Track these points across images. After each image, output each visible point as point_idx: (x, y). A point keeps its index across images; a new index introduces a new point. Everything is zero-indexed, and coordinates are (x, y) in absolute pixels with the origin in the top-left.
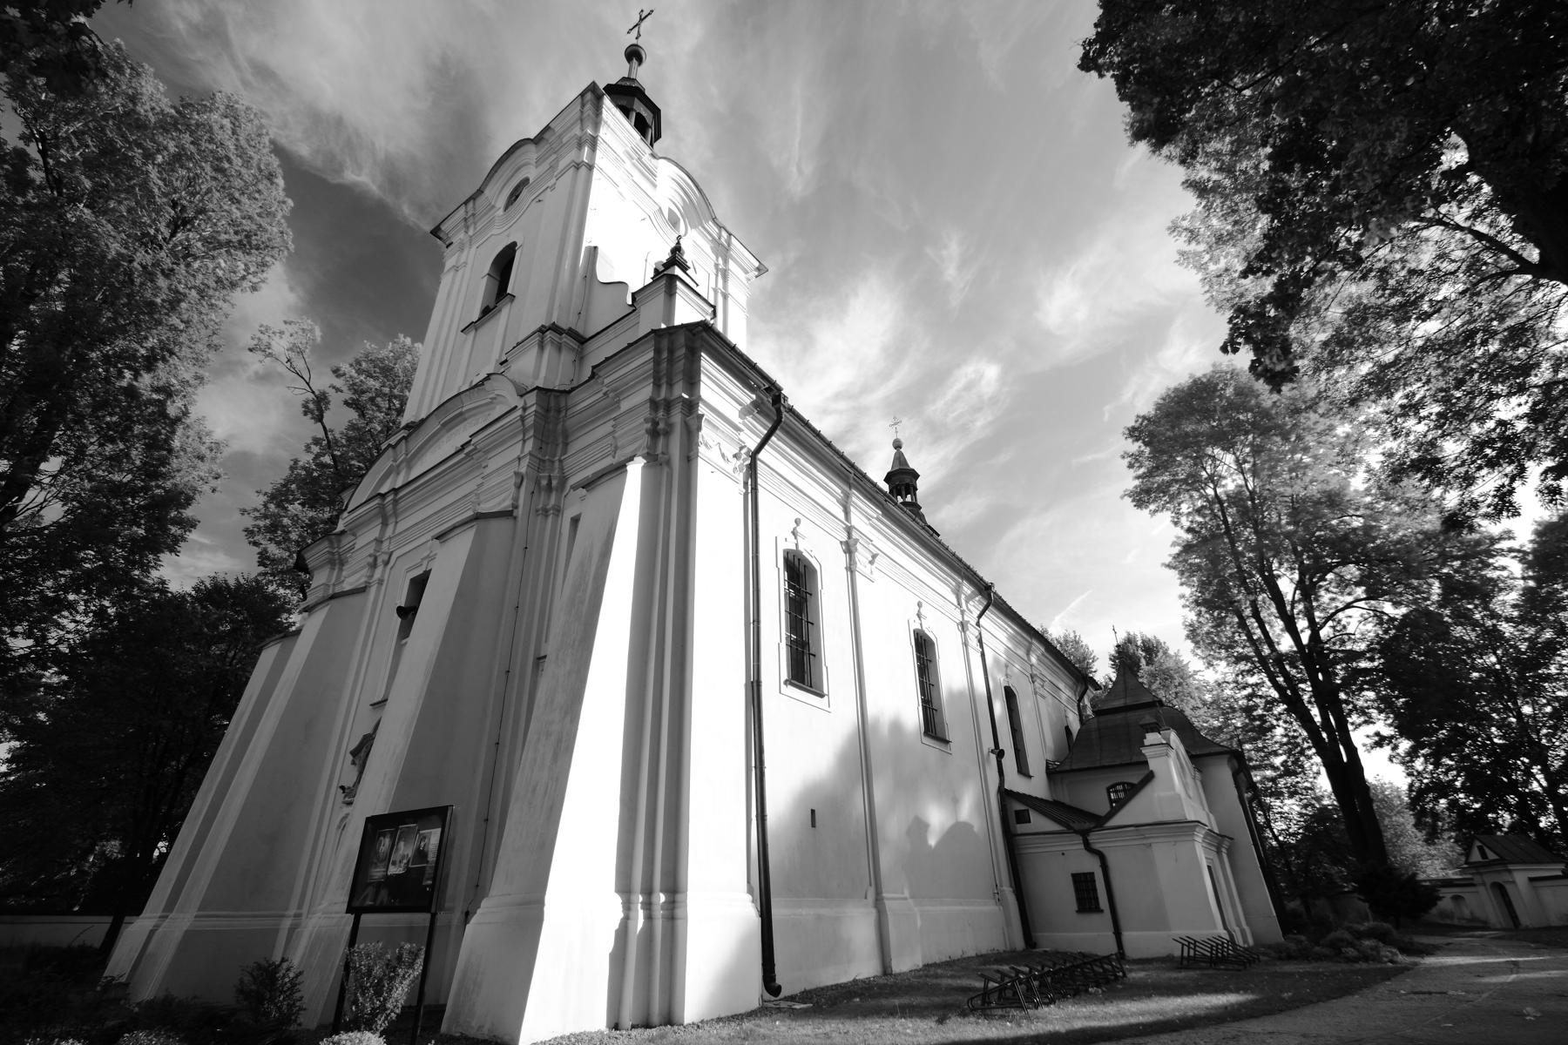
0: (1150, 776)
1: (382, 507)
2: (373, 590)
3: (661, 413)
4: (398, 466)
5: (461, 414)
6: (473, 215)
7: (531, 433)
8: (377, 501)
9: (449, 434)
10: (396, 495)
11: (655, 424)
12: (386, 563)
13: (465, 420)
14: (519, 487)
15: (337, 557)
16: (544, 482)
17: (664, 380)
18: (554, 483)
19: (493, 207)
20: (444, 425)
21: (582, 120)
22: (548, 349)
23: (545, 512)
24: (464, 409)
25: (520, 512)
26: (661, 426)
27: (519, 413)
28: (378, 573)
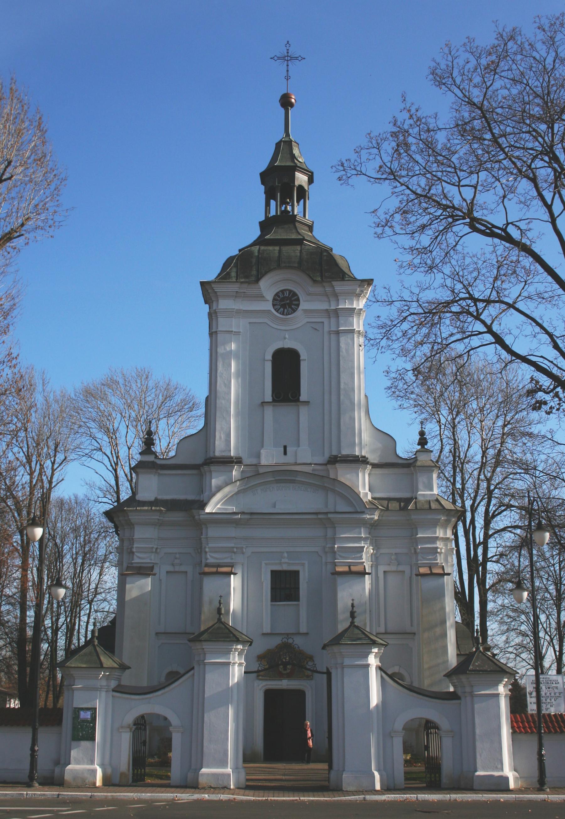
5: (295, 480)
13: (294, 483)
20: (276, 480)
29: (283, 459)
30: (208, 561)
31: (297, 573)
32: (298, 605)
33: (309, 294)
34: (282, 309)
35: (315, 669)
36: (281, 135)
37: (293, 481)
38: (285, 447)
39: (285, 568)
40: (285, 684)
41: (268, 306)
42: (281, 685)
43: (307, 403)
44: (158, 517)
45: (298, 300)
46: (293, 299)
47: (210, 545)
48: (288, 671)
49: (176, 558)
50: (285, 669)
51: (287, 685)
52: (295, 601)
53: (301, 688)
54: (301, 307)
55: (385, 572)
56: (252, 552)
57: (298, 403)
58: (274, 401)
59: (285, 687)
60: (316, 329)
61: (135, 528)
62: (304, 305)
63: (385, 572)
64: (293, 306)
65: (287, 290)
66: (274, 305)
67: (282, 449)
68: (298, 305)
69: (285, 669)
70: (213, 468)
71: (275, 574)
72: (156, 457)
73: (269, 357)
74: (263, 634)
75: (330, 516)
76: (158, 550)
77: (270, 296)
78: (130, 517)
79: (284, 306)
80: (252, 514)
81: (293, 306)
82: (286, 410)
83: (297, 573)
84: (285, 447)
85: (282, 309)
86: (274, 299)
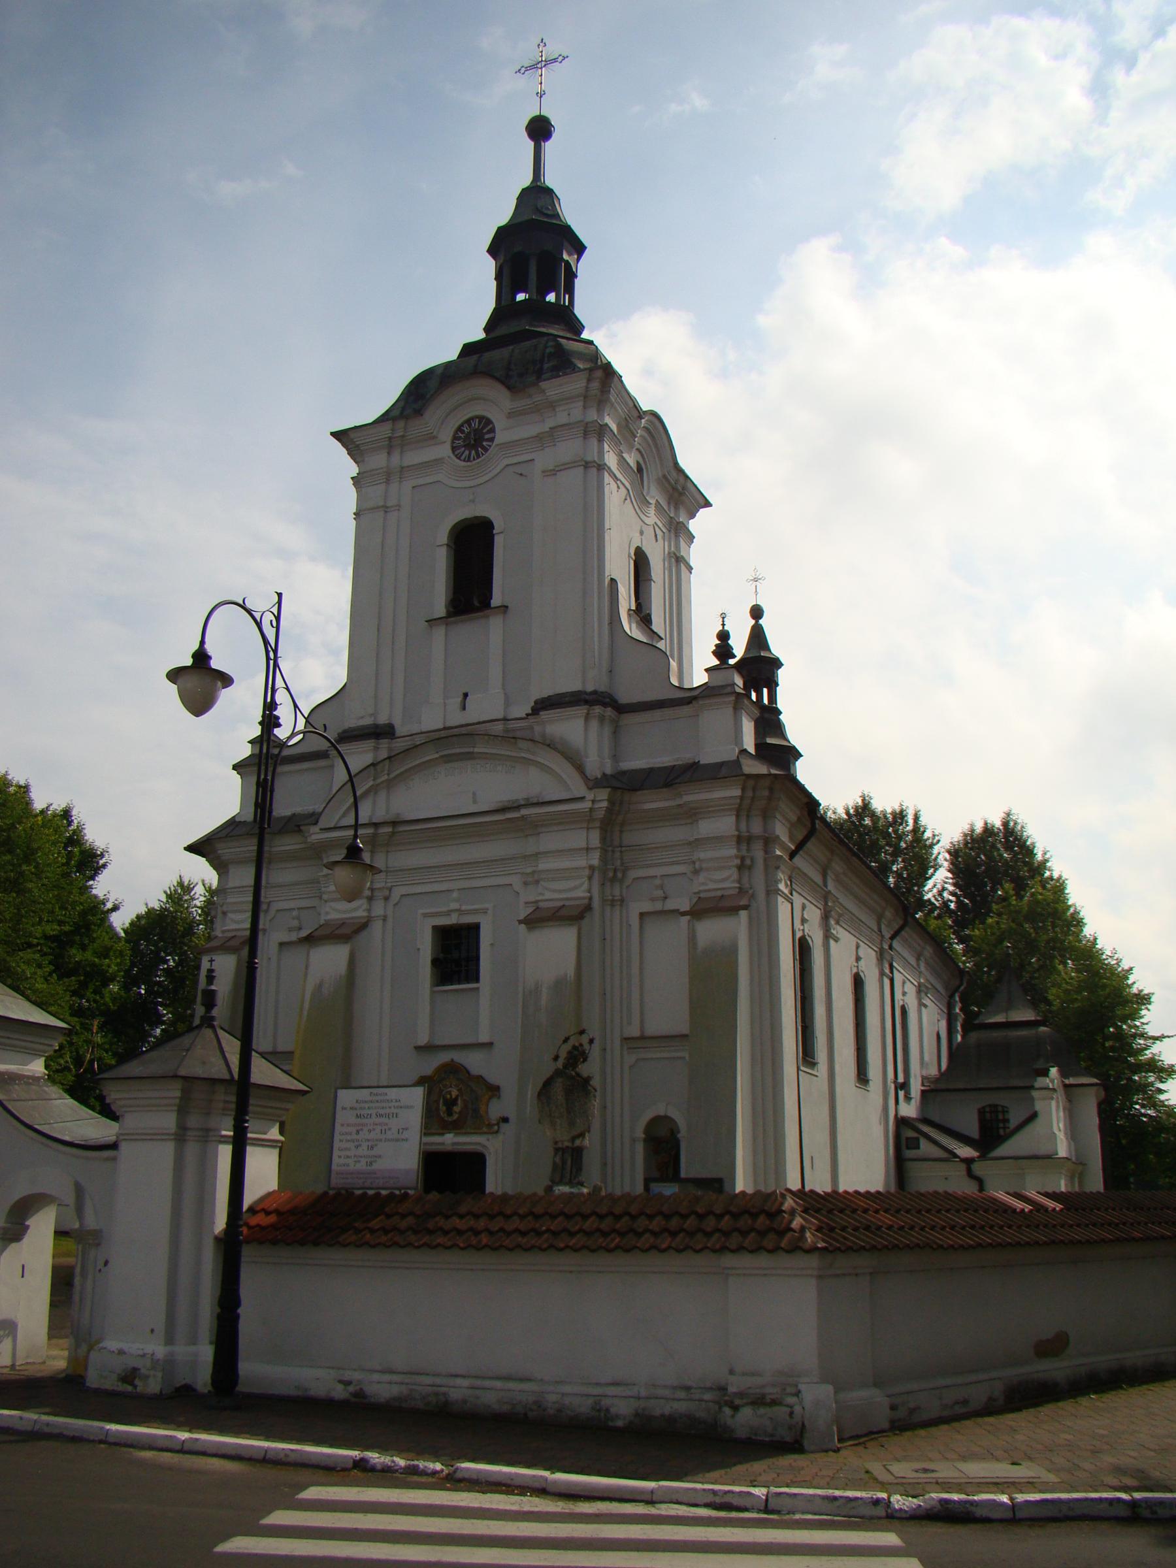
0: (1033, 1116)
1: (375, 835)
2: (377, 926)
3: (744, 847)
4: (378, 785)
5: (473, 753)
6: (403, 436)
7: (597, 824)
11: (743, 859)
12: (386, 899)
13: (474, 758)
14: (590, 878)
16: (611, 874)
18: (619, 875)
19: (435, 437)
21: (585, 397)
22: (594, 725)
23: (612, 903)
24: (476, 750)
25: (596, 904)
26: (748, 862)
27: (589, 804)
28: (378, 909)
29: (456, 718)
30: (329, 917)
32: (478, 989)
33: (510, 415)
34: (467, 452)
36: (526, 180)
37: (470, 756)
39: (453, 920)
40: (449, 1141)
41: (445, 451)
42: (443, 1144)
43: (504, 608)
45: (493, 430)
46: (485, 431)
48: (456, 1117)
49: (293, 918)
50: (450, 1112)
51: (454, 1144)
52: (468, 981)
53: (479, 1148)
54: (496, 441)
55: (642, 915)
56: (402, 896)
57: (487, 612)
58: (450, 615)
59: (449, 1148)
60: (521, 474)
61: (231, 871)
62: (501, 437)
63: (642, 915)
64: (484, 443)
65: (477, 417)
66: (454, 449)
68: (492, 440)
69: (450, 1112)
73: (443, 537)
74: (418, 1048)
75: (524, 812)
77: (447, 434)
78: (220, 852)
79: (468, 446)
80: (394, 823)
81: (484, 443)
82: (468, 630)
83: (476, 927)
85: (467, 452)
86: (455, 438)
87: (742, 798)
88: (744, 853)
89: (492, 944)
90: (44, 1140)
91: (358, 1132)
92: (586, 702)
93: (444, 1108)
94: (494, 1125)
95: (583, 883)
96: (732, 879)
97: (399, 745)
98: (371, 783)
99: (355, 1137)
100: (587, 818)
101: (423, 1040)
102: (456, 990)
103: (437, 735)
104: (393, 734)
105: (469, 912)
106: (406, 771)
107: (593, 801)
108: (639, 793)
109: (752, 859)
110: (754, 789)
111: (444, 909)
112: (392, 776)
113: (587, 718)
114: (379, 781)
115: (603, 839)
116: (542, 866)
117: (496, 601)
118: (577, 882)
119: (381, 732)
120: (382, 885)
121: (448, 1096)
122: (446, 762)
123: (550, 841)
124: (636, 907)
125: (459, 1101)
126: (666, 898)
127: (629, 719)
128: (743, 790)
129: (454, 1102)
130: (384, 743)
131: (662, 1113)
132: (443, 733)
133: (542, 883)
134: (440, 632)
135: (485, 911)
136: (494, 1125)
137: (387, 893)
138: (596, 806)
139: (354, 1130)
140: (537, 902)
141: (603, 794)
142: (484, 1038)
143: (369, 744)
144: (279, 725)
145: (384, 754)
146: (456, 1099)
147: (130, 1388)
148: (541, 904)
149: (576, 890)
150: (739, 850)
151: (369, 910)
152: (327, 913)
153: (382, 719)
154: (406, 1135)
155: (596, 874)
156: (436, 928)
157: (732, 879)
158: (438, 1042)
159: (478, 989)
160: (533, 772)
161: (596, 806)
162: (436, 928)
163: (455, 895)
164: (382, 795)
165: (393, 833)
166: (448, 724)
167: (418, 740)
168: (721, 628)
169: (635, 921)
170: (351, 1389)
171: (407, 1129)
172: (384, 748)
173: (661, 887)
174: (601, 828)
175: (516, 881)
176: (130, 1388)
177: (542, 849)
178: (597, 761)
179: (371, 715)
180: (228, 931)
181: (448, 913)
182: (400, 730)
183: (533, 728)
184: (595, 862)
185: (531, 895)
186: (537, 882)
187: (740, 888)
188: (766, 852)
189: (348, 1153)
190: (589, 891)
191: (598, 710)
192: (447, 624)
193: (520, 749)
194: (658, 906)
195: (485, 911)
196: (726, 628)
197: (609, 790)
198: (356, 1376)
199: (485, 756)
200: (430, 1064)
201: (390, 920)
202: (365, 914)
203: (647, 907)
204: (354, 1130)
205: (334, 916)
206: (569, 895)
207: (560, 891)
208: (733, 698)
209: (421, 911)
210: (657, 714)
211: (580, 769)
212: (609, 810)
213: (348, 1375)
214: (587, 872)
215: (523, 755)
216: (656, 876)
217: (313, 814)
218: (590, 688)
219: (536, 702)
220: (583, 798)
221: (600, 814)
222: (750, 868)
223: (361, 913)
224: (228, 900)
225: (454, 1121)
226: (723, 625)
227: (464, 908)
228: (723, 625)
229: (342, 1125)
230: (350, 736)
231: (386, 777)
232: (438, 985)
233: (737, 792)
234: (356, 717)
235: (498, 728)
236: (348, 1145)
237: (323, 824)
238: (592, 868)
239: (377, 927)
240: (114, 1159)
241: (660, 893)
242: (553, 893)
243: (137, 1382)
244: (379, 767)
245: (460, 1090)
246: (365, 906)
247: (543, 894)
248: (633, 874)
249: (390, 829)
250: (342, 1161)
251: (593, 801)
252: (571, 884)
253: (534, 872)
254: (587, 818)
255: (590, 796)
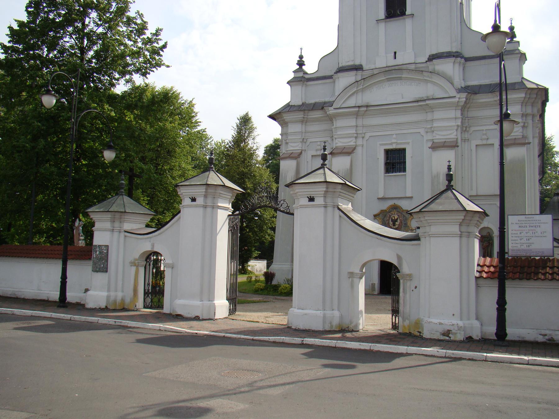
3: (524, 118)
8: (357, 109)
9: (389, 82)
10: (367, 108)
11: (524, 123)
12: (363, 138)
13: (401, 80)
14: (457, 130)
15: (305, 119)
16: (464, 129)
17: (525, 104)
18: (468, 129)
22: (457, 66)
24: (403, 76)
25: (459, 141)
26: (526, 125)
27: (457, 100)
28: (360, 142)
29: (392, 62)
30: (337, 145)
31: (404, 150)
32: (406, 175)
35: (288, 211)
37: (400, 79)
38: (395, 53)
39: (394, 147)
43: (412, 15)
44: (303, 116)
47: (339, 133)
48: (397, 226)
49: (318, 146)
63: (476, 145)
67: (393, 54)
70: (339, 75)
71: (388, 152)
72: (306, 73)
74: (378, 198)
75: (428, 102)
76: (305, 140)
80: (367, 106)
82: (396, 24)
83: (404, 150)
84: (395, 53)
87: (525, 98)
88: (524, 121)
89: (412, 157)
90: (379, 237)
91: (520, 233)
92: (454, 56)
93: (392, 223)
94: (414, 230)
95: (454, 133)
96: (519, 131)
97: (366, 74)
98: (356, 89)
99: (519, 235)
100: (456, 105)
101: (381, 196)
102: (395, 175)
103: (384, 70)
104: (363, 69)
105: (401, 144)
106: (371, 84)
107: (459, 98)
108: (477, 95)
109: (528, 123)
110: (530, 94)
111: (390, 142)
112: (364, 86)
113: (454, 63)
114: (359, 88)
115: (462, 114)
116: (435, 125)
117: (407, 13)
118: (452, 132)
119: (358, 68)
120: (361, 132)
121: (394, 218)
122: (388, 81)
123: (438, 114)
124: (474, 143)
125: (398, 220)
126: (488, 139)
127: (469, 64)
128: (526, 94)
129: (396, 220)
130: (360, 72)
131: (486, 226)
132: (387, 69)
133: (435, 132)
134: (382, 25)
135: (408, 143)
136: (414, 230)
137: (363, 135)
138: (460, 100)
139: (519, 232)
140: (433, 140)
141: (464, 95)
142: (408, 195)
143: (353, 73)
144: (304, 65)
145: (359, 78)
146: (397, 219)
147: (447, 338)
148: (435, 141)
149: (452, 135)
150: (522, 120)
151: (356, 142)
152: (336, 143)
153: (357, 63)
154: (545, 234)
155: (459, 129)
156: (384, 149)
157: (519, 131)
158: (387, 197)
159: (406, 175)
160: (430, 85)
161: (460, 100)
162: (384, 149)
163: (394, 136)
164: (360, 95)
165: (366, 110)
166: (389, 65)
167: (376, 72)
168: (510, 25)
169: (474, 148)
170: (547, 337)
171: (545, 232)
172: (359, 75)
173: (486, 134)
174: (461, 110)
175: (422, 131)
176: (447, 338)
177: (435, 118)
178: (459, 82)
179: (352, 61)
180: (289, 150)
181: (392, 144)
182: (365, 67)
183: (428, 67)
184: (459, 124)
185: (430, 136)
186: (433, 131)
187: (523, 135)
188: (533, 121)
189: (517, 242)
190: (456, 136)
191: (459, 59)
192: (385, 22)
193: (424, 75)
194: (485, 142)
195: (408, 143)
196: (512, 25)
197: (467, 93)
198: (547, 332)
199: (406, 79)
200: (385, 206)
201: (365, 146)
202: (354, 144)
203: (479, 142)
204: (519, 232)
205: (339, 144)
206: (445, 137)
207: (442, 135)
208: (519, 55)
209: (378, 143)
210: (483, 62)
211: (452, 84)
212: (465, 102)
213: (543, 332)
214: (456, 128)
215: (425, 78)
216: (483, 130)
217: (329, 102)
218: (454, 50)
219: (429, 56)
220: (455, 97)
221: (462, 104)
222: (526, 127)
223: (352, 143)
224: (289, 138)
225: (396, 228)
226: (511, 23)
227: (398, 142)
228: (511, 23)
229: (512, 230)
230: (342, 70)
231: (362, 87)
232: (386, 173)
233: (523, 95)
234: (346, 62)
235: (413, 67)
236: (516, 238)
237: (334, 106)
238: (458, 126)
239: (359, 150)
240: (419, 244)
241: (485, 137)
242: (440, 136)
243: (450, 335)
244: (359, 83)
245: (398, 216)
246: (354, 140)
247: (435, 137)
248: (473, 129)
249: (365, 109)
250: (514, 245)
251: (459, 98)
252: (449, 132)
253: (431, 127)
254: (456, 106)
255: (458, 96)
